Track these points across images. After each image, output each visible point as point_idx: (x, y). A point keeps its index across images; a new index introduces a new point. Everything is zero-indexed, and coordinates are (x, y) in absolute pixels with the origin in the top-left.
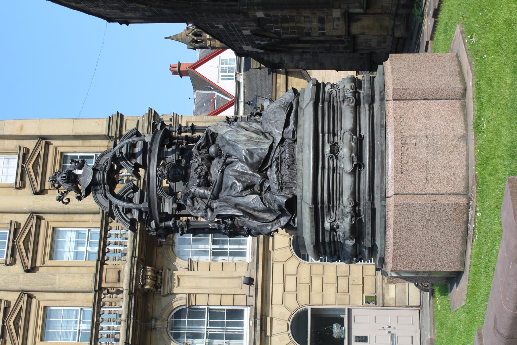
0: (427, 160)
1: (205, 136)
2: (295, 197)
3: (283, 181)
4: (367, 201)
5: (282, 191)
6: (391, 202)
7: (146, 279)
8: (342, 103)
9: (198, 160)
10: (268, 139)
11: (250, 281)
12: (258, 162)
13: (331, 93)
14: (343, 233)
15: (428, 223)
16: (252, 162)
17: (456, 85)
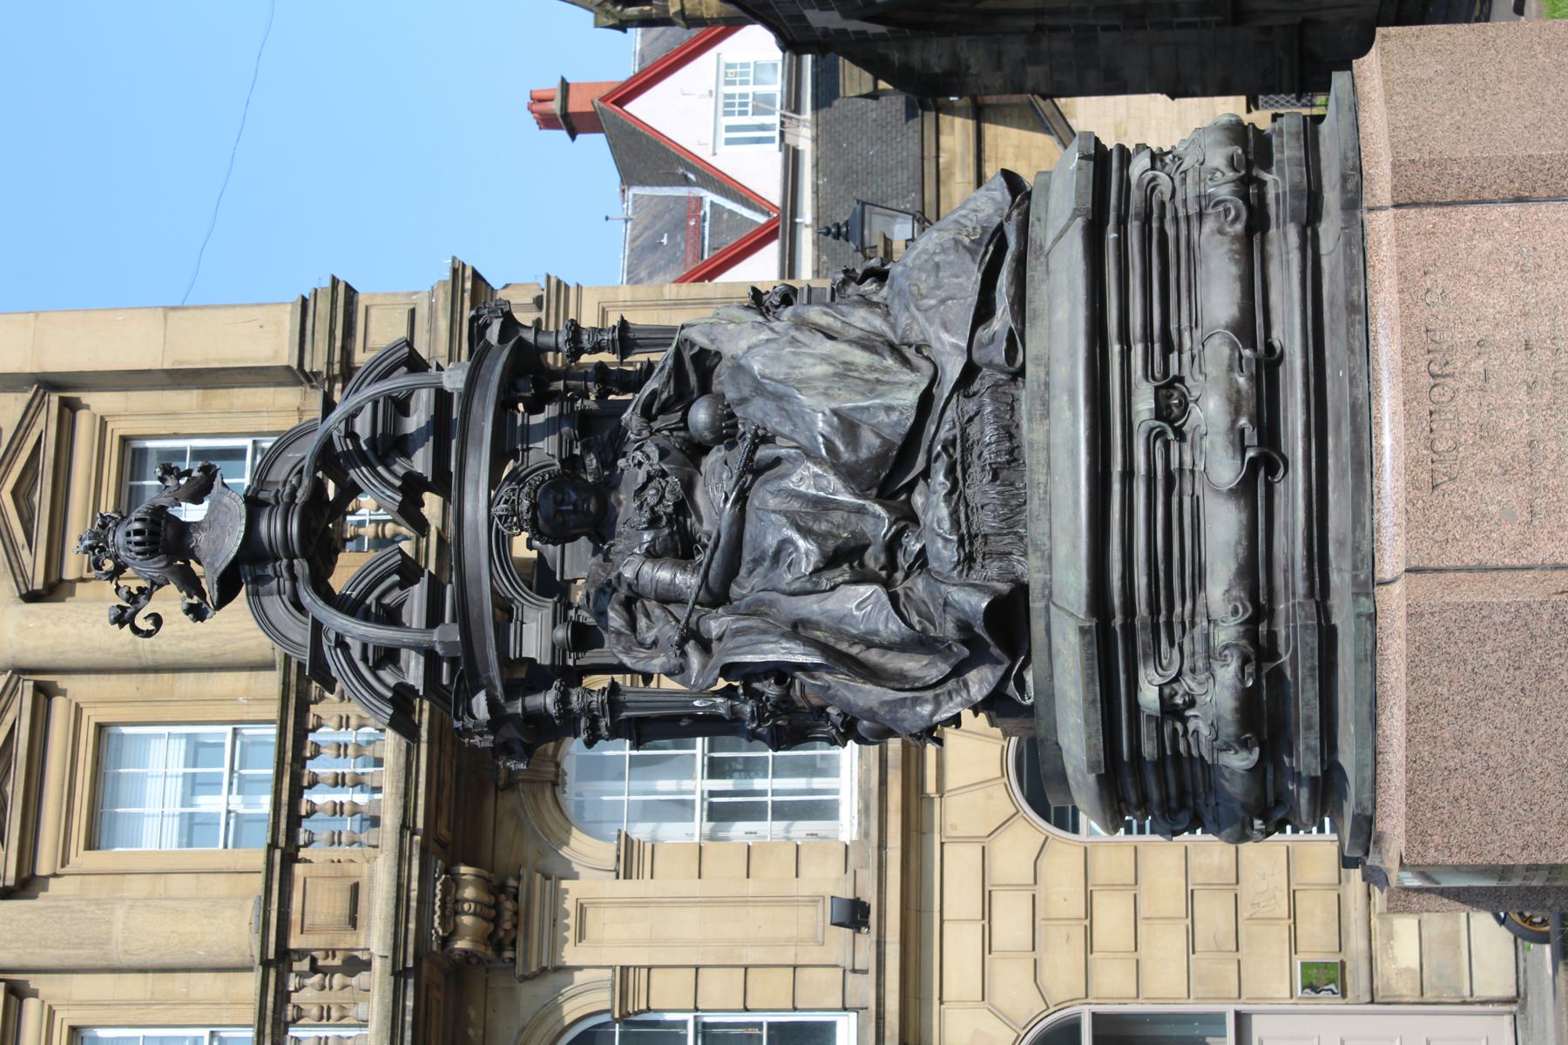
0: (1530, 434)
1: (670, 362)
2: (1021, 590)
3: (974, 529)
4: (1302, 600)
5: (970, 568)
6: (1393, 600)
7: (457, 913)
8: (1195, 224)
9: (648, 458)
11: (854, 915)
12: (878, 460)
13: (1152, 186)
14: (1212, 724)
15: (1540, 680)
16: (853, 458)
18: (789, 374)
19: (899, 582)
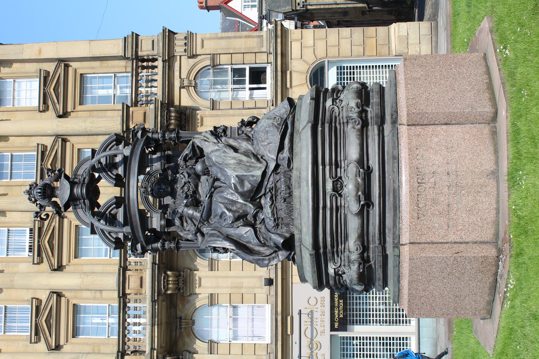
0: (448, 202)
1: (191, 147)
2: (292, 236)
4: (377, 245)
5: (278, 228)
6: (405, 251)
8: (346, 125)
9: (185, 177)
12: (250, 191)
13: (333, 111)
16: (243, 191)
17: (485, 107)
18: (223, 162)
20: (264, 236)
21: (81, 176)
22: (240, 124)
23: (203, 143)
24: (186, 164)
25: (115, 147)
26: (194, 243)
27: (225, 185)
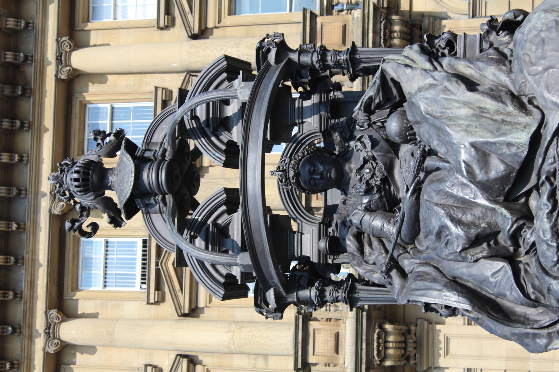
1: (378, 82)
9: (365, 147)
10: (527, 113)
12: (503, 179)
16: (486, 178)
18: (442, 113)
19: (522, 255)
20: (537, 283)
21: (159, 145)
22: (486, 27)
23: (402, 72)
24: (369, 119)
25: (226, 83)
26: (387, 291)
27: (447, 165)
